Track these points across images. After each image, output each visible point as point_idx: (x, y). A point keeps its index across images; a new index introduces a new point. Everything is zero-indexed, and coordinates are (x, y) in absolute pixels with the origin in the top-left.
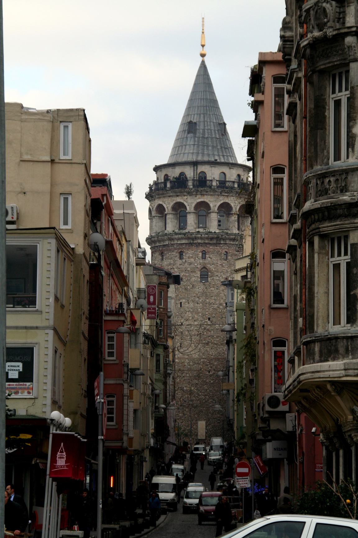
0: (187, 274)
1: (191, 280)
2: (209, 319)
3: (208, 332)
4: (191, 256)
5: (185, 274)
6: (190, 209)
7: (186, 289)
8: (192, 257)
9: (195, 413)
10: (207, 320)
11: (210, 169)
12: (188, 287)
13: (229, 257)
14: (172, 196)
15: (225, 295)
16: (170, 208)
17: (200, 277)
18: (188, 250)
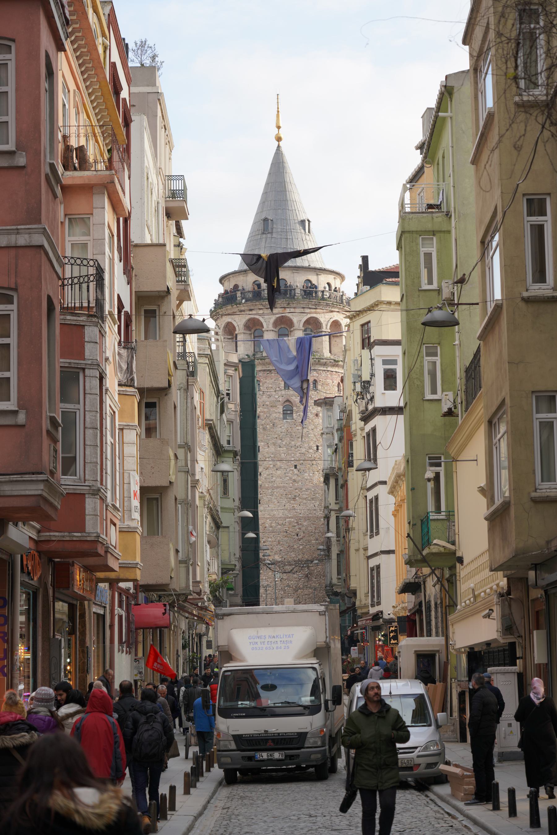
0: (265, 410)
1: (271, 417)
2: (296, 467)
3: (294, 483)
4: (270, 386)
5: (262, 410)
6: (268, 325)
7: (264, 429)
8: (272, 388)
9: (280, 588)
10: (293, 468)
11: (292, 275)
12: (268, 426)
13: (319, 387)
14: (244, 311)
15: (315, 436)
16: (242, 326)
17: (283, 414)
18: (266, 378)
